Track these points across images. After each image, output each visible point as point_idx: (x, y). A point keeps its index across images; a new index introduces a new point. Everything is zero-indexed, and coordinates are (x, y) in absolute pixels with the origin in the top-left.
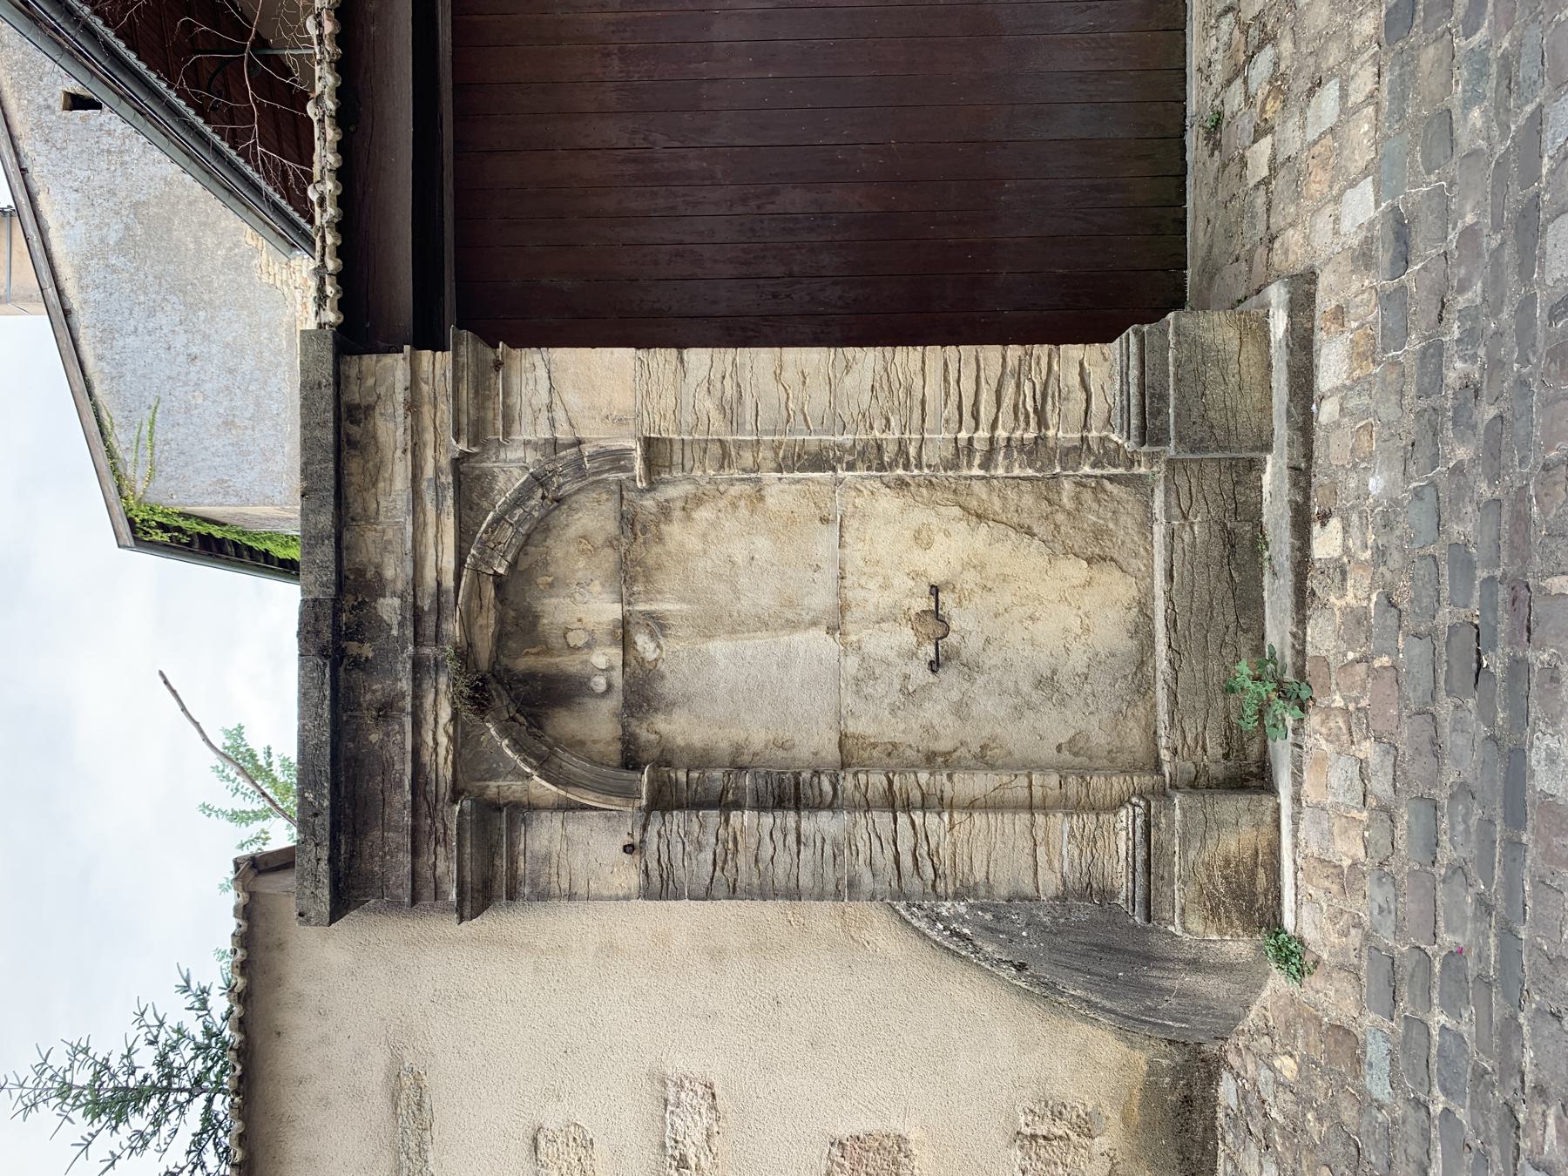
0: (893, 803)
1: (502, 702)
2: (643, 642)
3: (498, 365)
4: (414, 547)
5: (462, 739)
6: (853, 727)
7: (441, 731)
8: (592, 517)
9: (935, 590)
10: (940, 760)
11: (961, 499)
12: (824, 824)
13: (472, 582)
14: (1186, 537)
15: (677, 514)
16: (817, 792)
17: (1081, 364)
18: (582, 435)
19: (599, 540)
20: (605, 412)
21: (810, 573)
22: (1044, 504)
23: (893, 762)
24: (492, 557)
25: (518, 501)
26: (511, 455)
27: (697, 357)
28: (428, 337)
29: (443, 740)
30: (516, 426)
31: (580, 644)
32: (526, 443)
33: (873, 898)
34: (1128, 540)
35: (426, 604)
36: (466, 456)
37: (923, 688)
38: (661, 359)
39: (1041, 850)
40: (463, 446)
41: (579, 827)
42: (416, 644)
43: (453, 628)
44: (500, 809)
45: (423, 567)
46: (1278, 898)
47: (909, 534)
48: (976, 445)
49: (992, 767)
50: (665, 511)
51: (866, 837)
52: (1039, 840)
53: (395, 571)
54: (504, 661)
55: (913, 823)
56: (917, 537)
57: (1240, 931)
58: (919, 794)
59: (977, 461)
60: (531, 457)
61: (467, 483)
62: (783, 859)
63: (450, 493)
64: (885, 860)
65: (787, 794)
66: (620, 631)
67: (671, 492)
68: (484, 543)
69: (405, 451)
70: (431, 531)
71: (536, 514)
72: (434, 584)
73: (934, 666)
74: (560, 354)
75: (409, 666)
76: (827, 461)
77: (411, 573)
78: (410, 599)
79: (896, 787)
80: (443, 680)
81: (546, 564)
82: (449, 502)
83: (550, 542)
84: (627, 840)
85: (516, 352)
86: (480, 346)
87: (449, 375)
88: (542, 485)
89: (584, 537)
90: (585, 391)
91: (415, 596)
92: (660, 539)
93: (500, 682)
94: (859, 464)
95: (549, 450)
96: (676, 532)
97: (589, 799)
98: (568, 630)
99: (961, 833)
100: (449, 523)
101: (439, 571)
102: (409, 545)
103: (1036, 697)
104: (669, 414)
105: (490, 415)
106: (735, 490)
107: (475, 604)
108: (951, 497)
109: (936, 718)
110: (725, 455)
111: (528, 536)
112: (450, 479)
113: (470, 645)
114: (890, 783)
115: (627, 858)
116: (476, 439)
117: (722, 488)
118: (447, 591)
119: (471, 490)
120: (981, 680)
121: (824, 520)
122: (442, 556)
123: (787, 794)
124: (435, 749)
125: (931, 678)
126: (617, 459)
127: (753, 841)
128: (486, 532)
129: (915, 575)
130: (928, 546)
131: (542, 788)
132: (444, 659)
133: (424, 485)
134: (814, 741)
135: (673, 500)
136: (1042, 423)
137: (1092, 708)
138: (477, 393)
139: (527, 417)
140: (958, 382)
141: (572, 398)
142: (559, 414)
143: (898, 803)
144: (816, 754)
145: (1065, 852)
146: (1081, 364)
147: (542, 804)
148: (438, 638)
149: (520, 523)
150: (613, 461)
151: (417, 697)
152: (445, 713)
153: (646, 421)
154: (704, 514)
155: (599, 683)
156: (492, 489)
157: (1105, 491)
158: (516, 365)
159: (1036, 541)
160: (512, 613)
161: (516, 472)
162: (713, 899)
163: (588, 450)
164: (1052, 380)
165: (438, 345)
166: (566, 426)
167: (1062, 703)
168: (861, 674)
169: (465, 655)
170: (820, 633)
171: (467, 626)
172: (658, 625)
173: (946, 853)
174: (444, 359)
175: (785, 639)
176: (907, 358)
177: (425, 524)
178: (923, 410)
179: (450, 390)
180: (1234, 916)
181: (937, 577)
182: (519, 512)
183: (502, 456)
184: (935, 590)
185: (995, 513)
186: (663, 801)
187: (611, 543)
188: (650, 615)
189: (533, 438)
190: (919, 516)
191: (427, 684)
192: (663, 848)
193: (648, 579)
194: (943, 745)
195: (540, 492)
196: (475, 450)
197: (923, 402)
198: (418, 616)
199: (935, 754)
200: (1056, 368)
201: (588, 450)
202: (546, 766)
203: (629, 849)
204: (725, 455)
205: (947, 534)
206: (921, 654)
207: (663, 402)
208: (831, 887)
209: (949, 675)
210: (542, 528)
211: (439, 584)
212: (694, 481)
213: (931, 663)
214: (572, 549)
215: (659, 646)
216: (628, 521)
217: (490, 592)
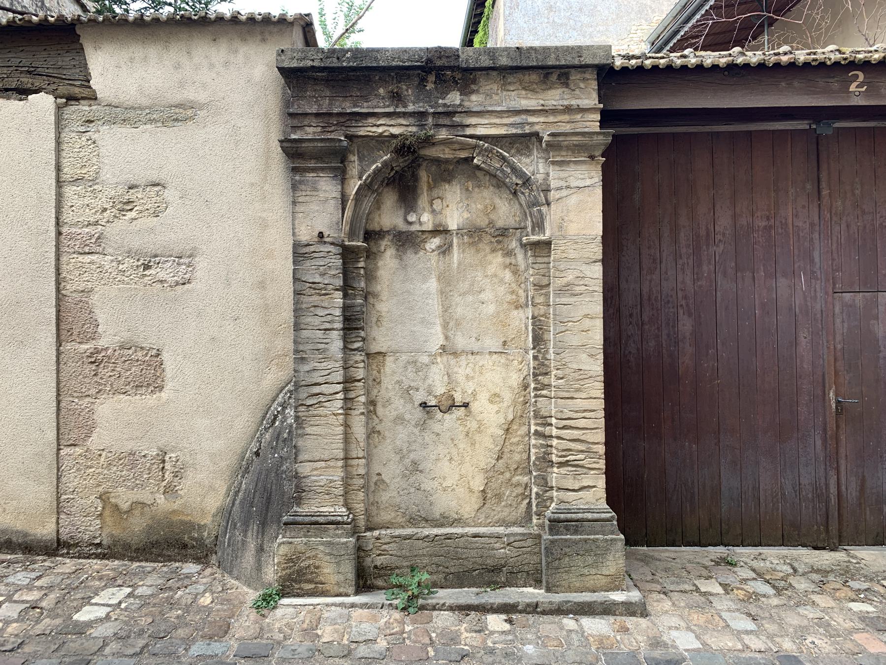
0: (348, 382)
1: (402, 162)
2: (436, 242)
3: (592, 157)
4: (488, 112)
5: (381, 141)
6: (389, 360)
7: (386, 128)
8: (505, 211)
9: (466, 405)
11: (517, 420)
12: (336, 345)
13: (469, 145)
14: (497, 545)
15: (508, 260)
16: (353, 340)
17: (594, 487)
18: (553, 206)
19: (492, 216)
20: (566, 218)
21: (475, 335)
24: (483, 156)
25: (514, 170)
26: (541, 166)
27: (597, 271)
28: (608, 118)
30: (557, 168)
31: (434, 206)
32: (548, 174)
33: (296, 371)
35: (457, 119)
36: (540, 139)
37: (411, 399)
38: (596, 249)
39: (323, 464)
40: (546, 138)
41: (332, 206)
42: (434, 113)
43: (443, 134)
44: (342, 162)
45: (477, 117)
46: (298, 596)
47: (497, 390)
48: (548, 428)
49: (368, 437)
50: (509, 253)
51: (329, 367)
53: (475, 101)
54: (425, 164)
56: (496, 395)
57: (279, 574)
58: (353, 396)
59: (539, 428)
60: (540, 177)
61: (525, 141)
62: (316, 321)
63: (519, 131)
64: (316, 378)
65: (352, 323)
67: (520, 257)
68: (491, 151)
69: (543, 105)
70: (498, 121)
71: (507, 180)
72: (468, 123)
73: (424, 405)
74: (599, 192)
75: (422, 109)
76: (538, 344)
77: (474, 110)
78: (459, 110)
79: (357, 384)
80: (414, 129)
81: (479, 187)
82: (514, 131)
83: (491, 188)
84: (326, 234)
85: (599, 168)
86: (603, 147)
87: (586, 130)
88: (524, 183)
91: (461, 112)
92: (493, 251)
93: (413, 161)
94: (537, 363)
95: (544, 187)
96: (498, 259)
97: (348, 213)
98: (442, 199)
99: (332, 420)
100: (502, 131)
101: (475, 126)
102: (490, 109)
103: (407, 461)
104: (565, 255)
105: (564, 153)
107: (456, 146)
109: (395, 406)
110: (542, 287)
111: (495, 176)
112: (527, 131)
113: (434, 144)
114: (359, 381)
115: (316, 234)
116: (549, 144)
117: (522, 285)
118: (464, 131)
119: (521, 143)
120: (416, 431)
121: (505, 343)
122: (484, 128)
123: (352, 323)
125: (417, 403)
126: (539, 226)
127: (326, 304)
128: (498, 152)
129: (474, 394)
130: (491, 402)
131: (354, 186)
132: (425, 129)
133: (524, 117)
134: (381, 338)
135: (516, 258)
136: (561, 465)
137: (401, 493)
138: (576, 145)
139: (563, 175)
141: (573, 200)
142: (564, 193)
143: (348, 385)
144: (374, 339)
145: (322, 477)
146: (594, 487)
147: (345, 186)
148: (437, 126)
149: (503, 171)
150: (538, 223)
151: (404, 115)
152: (395, 131)
153: (561, 242)
154: (508, 275)
155: (412, 218)
156: (521, 155)
157: (523, 500)
158: (592, 167)
159: (494, 462)
160: (451, 168)
161: (531, 169)
162: (294, 282)
163: (544, 209)
164: (585, 470)
165: (603, 123)
166: (557, 196)
167: (404, 476)
168: (419, 364)
169: (428, 141)
170: (441, 341)
171: (444, 142)
172: (445, 250)
173: (321, 411)
174: (595, 127)
175: (438, 321)
176: (597, 389)
177: (501, 118)
178: (568, 398)
179: (578, 130)
180: (288, 571)
181: (474, 406)
182: (509, 170)
183: (541, 161)
184: (466, 405)
185: (510, 439)
186: (348, 254)
187: (491, 223)
188: (451, 245)
189: (551, 178)
190: (508, 396)
191: (411, 120)
193: (471, 244)
194: (380, 410)
195: (520, 182)
196: (544, 145)
197: (572, 398)
198: (450, 114)
199: (375, 405)
200: (592, 472)
201: (544, 209)
202: (366, 188)
203: (321, 235)
204: (542, 287)
205: (498, 412)
206: (430, 397)
207: (572, 251)
208: (301, 348)
209: (419, 413)
210: (499, 183)
211: (468, 126)
213: (425, 403)
214: (488, 201)
215: (433, 251)
216: (503, 233)
217: (463, 155)
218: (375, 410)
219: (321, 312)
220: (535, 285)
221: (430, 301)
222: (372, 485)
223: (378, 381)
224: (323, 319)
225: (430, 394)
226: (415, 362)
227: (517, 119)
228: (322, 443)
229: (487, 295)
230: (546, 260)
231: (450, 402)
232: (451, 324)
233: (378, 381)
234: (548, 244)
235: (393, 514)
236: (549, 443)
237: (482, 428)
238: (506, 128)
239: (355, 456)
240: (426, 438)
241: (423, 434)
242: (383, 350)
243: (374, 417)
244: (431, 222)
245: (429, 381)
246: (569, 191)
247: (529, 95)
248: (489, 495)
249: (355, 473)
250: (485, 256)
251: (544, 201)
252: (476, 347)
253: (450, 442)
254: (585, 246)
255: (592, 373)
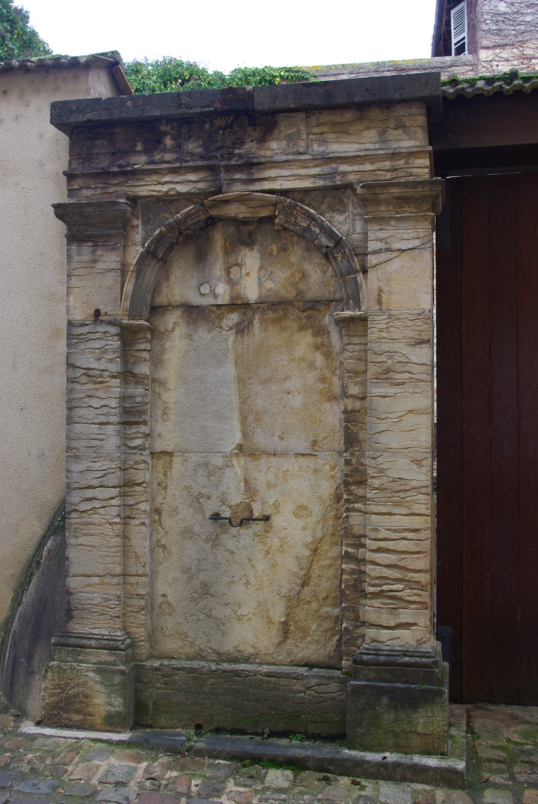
0: (127, 485)
2: (234, 318)
6: (177, 461)
7: (172, 186)
8: (317, 278)
9: (266, 518)
10: (157, 517)
11: (328, 538)
12: (112, 442)
14: (297, 687)
15: (319, 340)
16: (134, 436)
17: (415, 624)
18: (371, 274)
19: (302, 286)
20: (385, 289)
21: (278, 433)
22: (324, 595)
23: (155, 487)
28: (440, 163)
29: (165, 188)
31: (232, 275)
33: (68, 471)
34: (299, 649)
37: (202, 508)
39: (97, 580)
41: (112, 279)
46: (66, 727)
47: (304, 502)
48: (361, 550)
49: (152, 551)
50: (320, 332)
51: (104, 468)
52: (104, 579)
53: (275, 147)
55: (112, 498)
56: (302, 507)
57: (47, 701)
58: (132, 502)
59: (350, 550)
61: (336, 193)
62: (90, 414)
63: (329, 183)
64: (90, 479)
65: (131, 416)
66: (240, 302)
67: (335, 336)
70: (303, 172)
72: (267, 176)
73: (216, 517)
76: (352, 446)
79: (138, 488)
82: (321, 183)
84: (103, 311)
88: (336, 246)
89: (304, 276)
90: (405, 277)
92: (302, 328)
94: (349, 468)
95: (360, 251)
96: (305, 340)
97: (129, 287)
98: (240, 265)
99: (108, 530)
101: (275, 179)
103: (196, 583)
106: (336, 381)
108: (330, 532)
109: (180, 516)
110: (356, 373)
112: (338, 183)
114: (139, 485)
115: (92, 312)
117: (337, 372)
120: (207, 546)
121: (315, 443)
122: (283, 179)
123: (131, 416)
124: (160, 183)
125: (208, 514)
126: (354, 297)
127: (101, 394)
129: (276, 506)
130: (297, 516)
131: (135, 253)
133: (334, 166)
134: (168, 434)
135: (329, 338)
136: (375, 595)
137: (190, 619)
138: (397, 198)
140: (404, 539)
141: (396, 264)
142: (383, 257)
143: (127, 489)
144: (160, 435)
145: (95, 595)
146: (415, 624)
147: (127, 255)
153: (379, 318)
154: (319, 359)
155: (206, 289)
156: (333, 211)
157: (333, 635)
159: (298, 588)
162: (67, 368)
164: (405, 604)
166: (375, 262)
167: (193, 599)
168: (211, 467)
170: (238, 438)
172: (241, 329)
173: (96, 518)
175: (236, 415)
176: (424, 504)
177: (307, 168)
178: (384, 514)
180: (55, 698)
181: (277, 521)
182: (317, 231)
183: (357, 218)
184: (266, 518)
185: (318, 561)
186: (128, 336)
187: (300, 293)
188: (251, 323)
190: (317, 509)
192: (97, 336)
193: (276, 321)
194: (166, 520)
195: (331, 245)
197: (390, 514)
199: (160, 514)
200: (413, 606)
202: (149, 255)
203: (97, 313)
204: (356, 373)
205: (304, 528)
206: (223, 507)
208: (74, 444)
209: (210, 527)
210: (311, 246)
212: (343, 350)
213: (218, 514)
215: (231, 329)
216: (312, 307)
217: (264, 213)
218: (160, 520)
219: (95, 403)
220: (349, 371)
221: (224, 390)
222: (157, 607)
223: (164, 485)
224: (100, 411)
225: (224, 504)
226: (207, 464)
227: (326, 169)
228: (91, 557)
229: (294, 384)
230: (362, 340)
231: (246, 514)
232: (250, 418)
233: (164, 485)
234: (363, 320)
235: (180, 643)
236: (362, 568)
237: (285, 547)
238: (312, 180)
239: (134, 573)
240: (219, 556)
241: (215, 551)
242: (169, 449)
243: (159, 527)
244: (227, 294)
245: (223, 488)
246: (389, 255)
247: (341, 139)
248: (292, 628)
249: (134, 593)
250: (292, 335)
251: (358, 268)
252: (280, 446)
253: (246, 561)
254: (409, 323)
255: (414, 484)
